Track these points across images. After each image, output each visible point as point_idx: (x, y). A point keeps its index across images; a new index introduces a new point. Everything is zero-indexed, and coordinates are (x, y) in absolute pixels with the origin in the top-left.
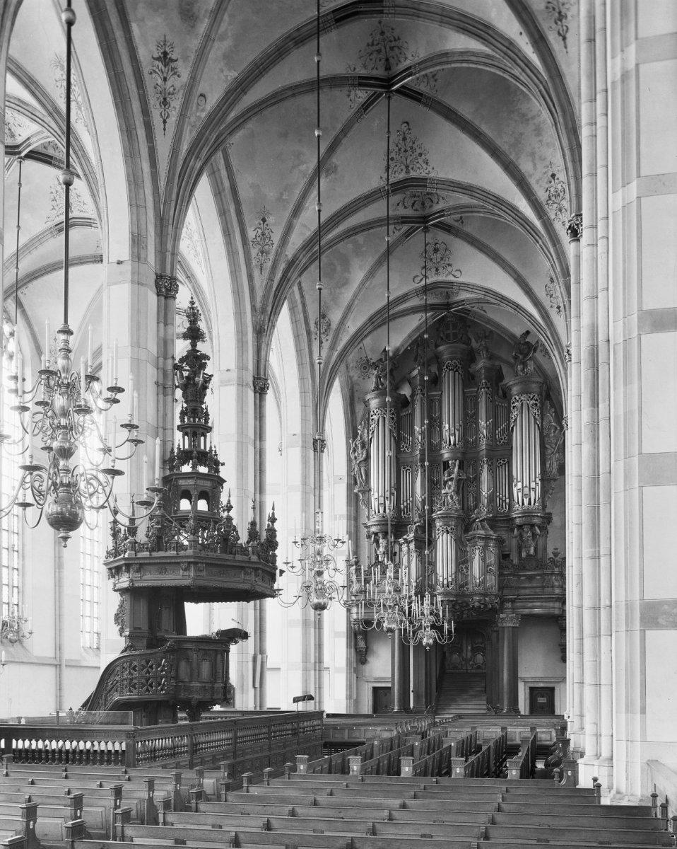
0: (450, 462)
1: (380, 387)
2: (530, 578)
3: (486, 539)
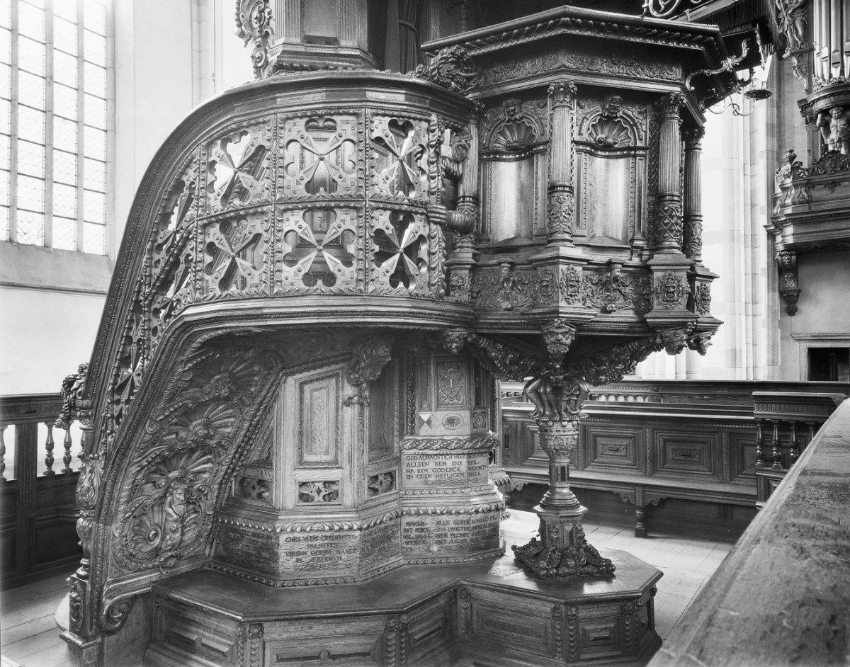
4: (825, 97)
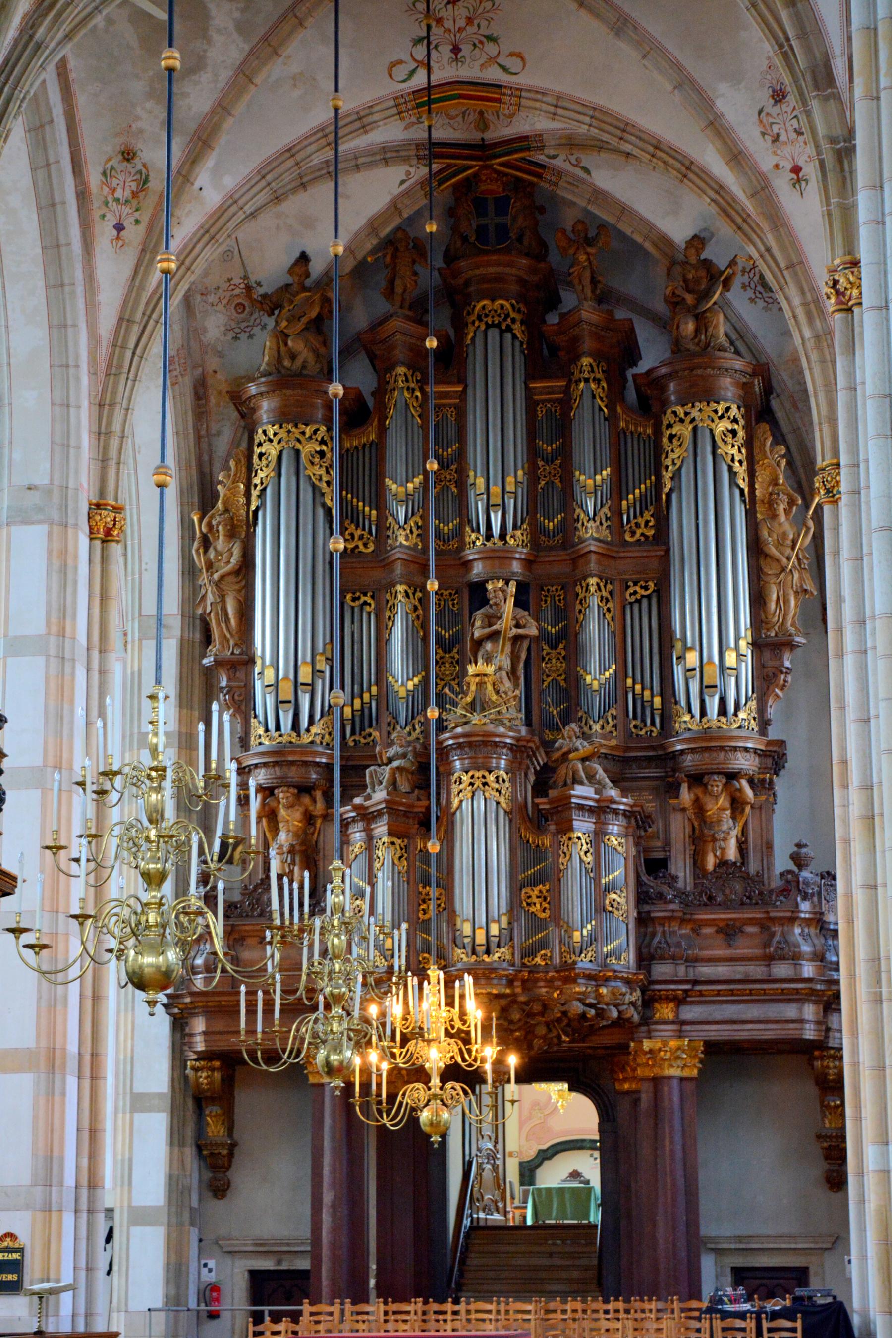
0: (490, 587)
1: (287, 363)
2: (729, 932)
3: (601, 810)
4: (265, 765)
